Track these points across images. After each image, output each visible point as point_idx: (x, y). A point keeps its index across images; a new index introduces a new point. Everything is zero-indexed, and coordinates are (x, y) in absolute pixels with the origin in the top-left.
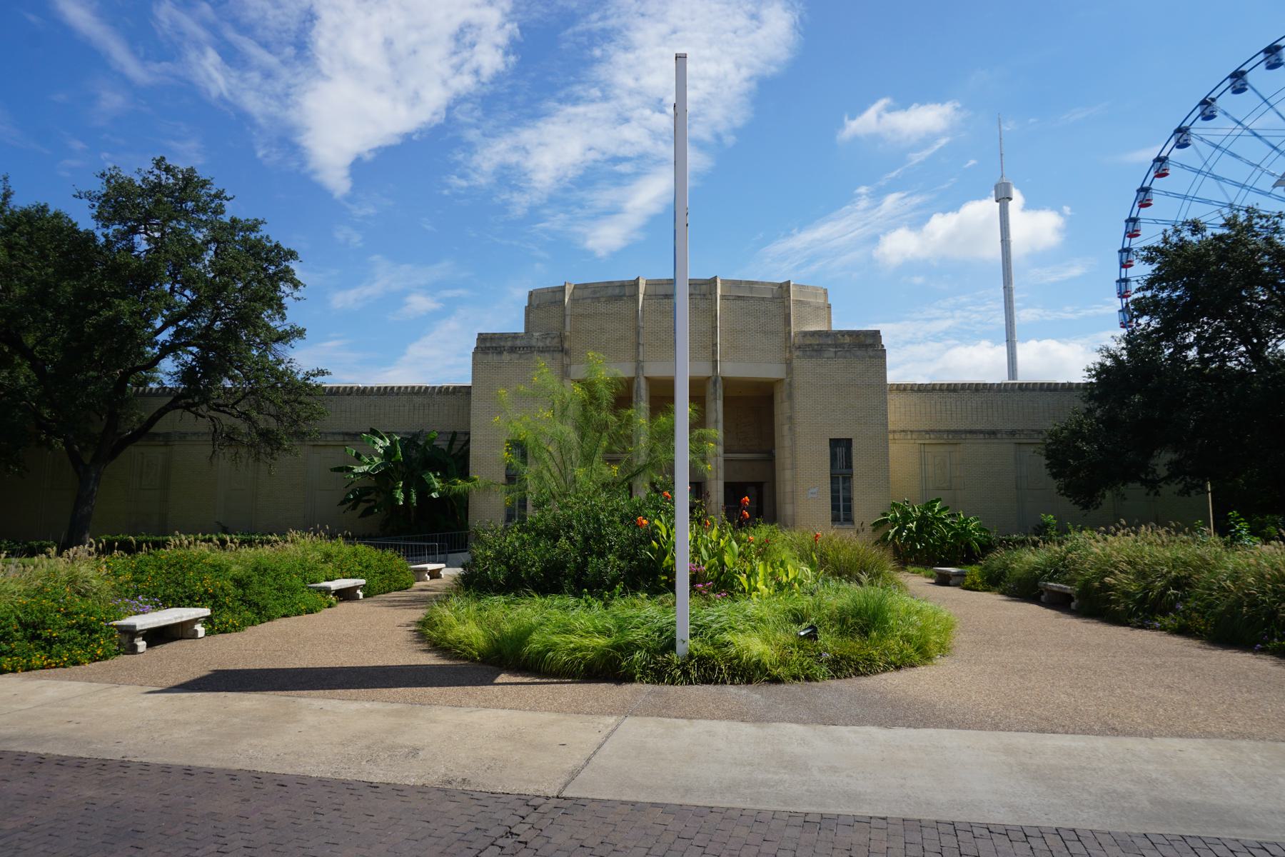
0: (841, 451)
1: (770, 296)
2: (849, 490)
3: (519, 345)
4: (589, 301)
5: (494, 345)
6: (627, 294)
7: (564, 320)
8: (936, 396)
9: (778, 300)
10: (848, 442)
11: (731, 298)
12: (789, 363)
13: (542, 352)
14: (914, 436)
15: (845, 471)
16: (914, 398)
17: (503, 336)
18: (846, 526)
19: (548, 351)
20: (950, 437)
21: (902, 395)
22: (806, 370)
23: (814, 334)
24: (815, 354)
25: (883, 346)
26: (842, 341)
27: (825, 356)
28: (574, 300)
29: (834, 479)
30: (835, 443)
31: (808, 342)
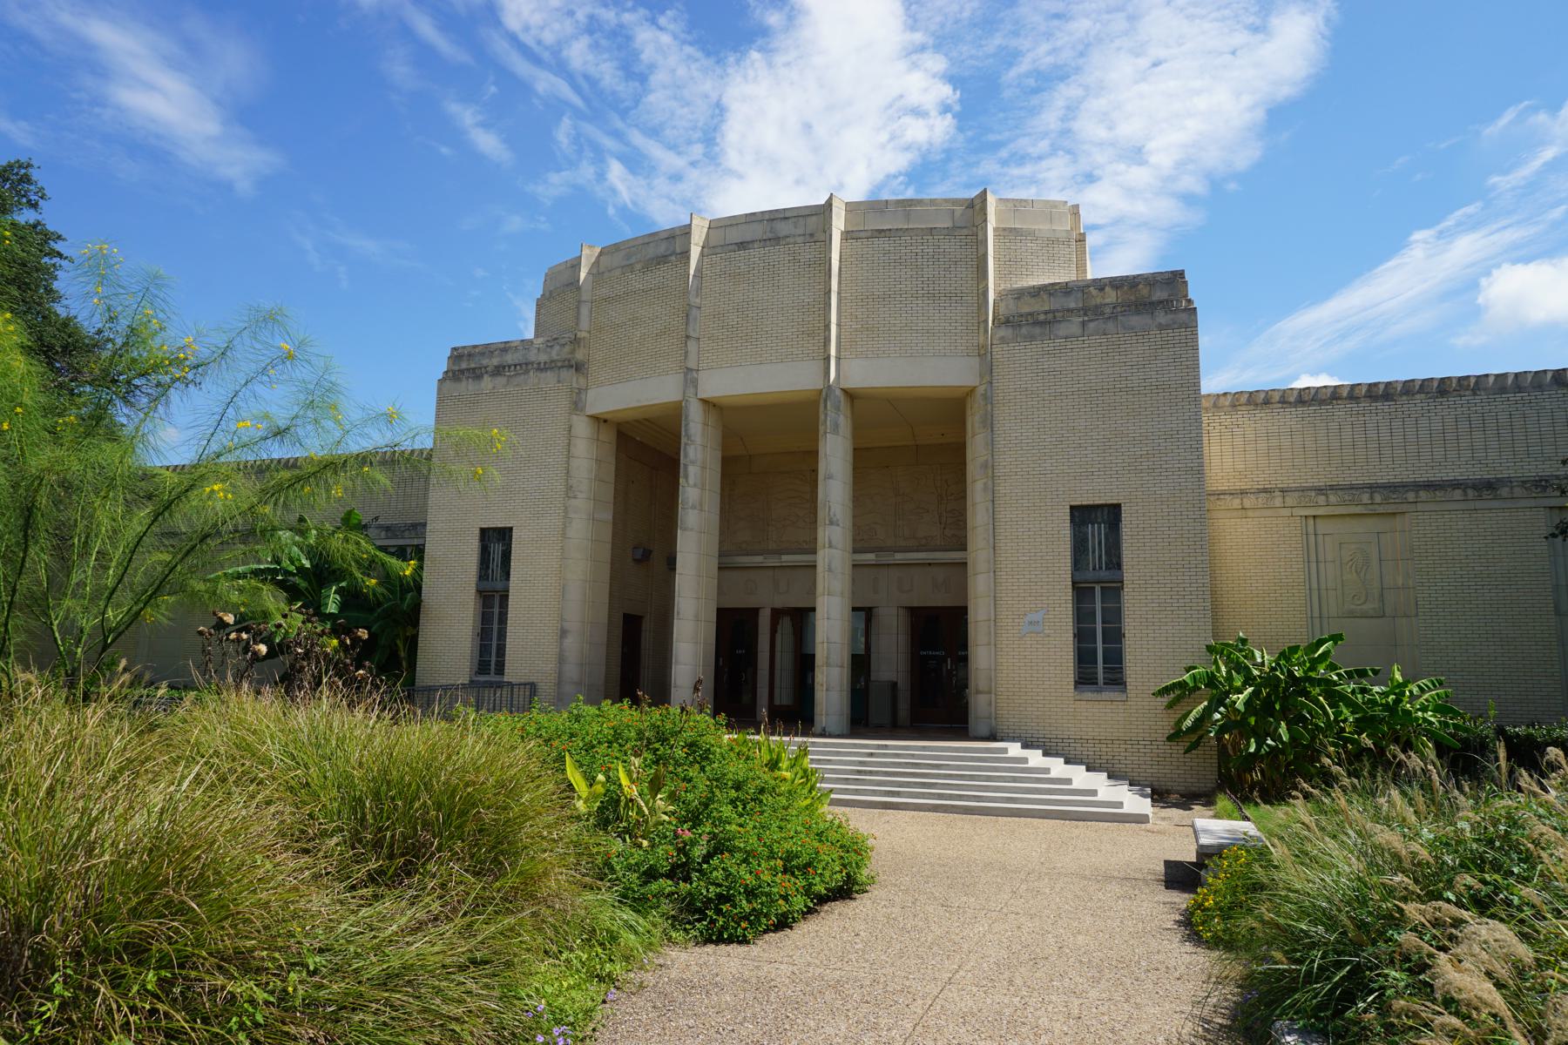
0: (1096, 533)
1: (949, 224)
2: (1114, 617)
3: (510, 362)
5: (473, 366)
6: (678, 251)
7: (578, 313)
8: (1340, 411)
9: (965, 232)
10: (1112, 514)
11: (863, 235)
14: (1290, 501)
16: (1290, 418)
17: (488, 350)
18: (1106, 695)
21: (1259, 414)
23: (1037, 292)
24: (1037, 330)
25: (1190, 301)
26: (1099, 301)
27: (1061, 333)
28: (597, 271)
29: (1081, 592)
30: (1081, 515)
31: (1026, 309)
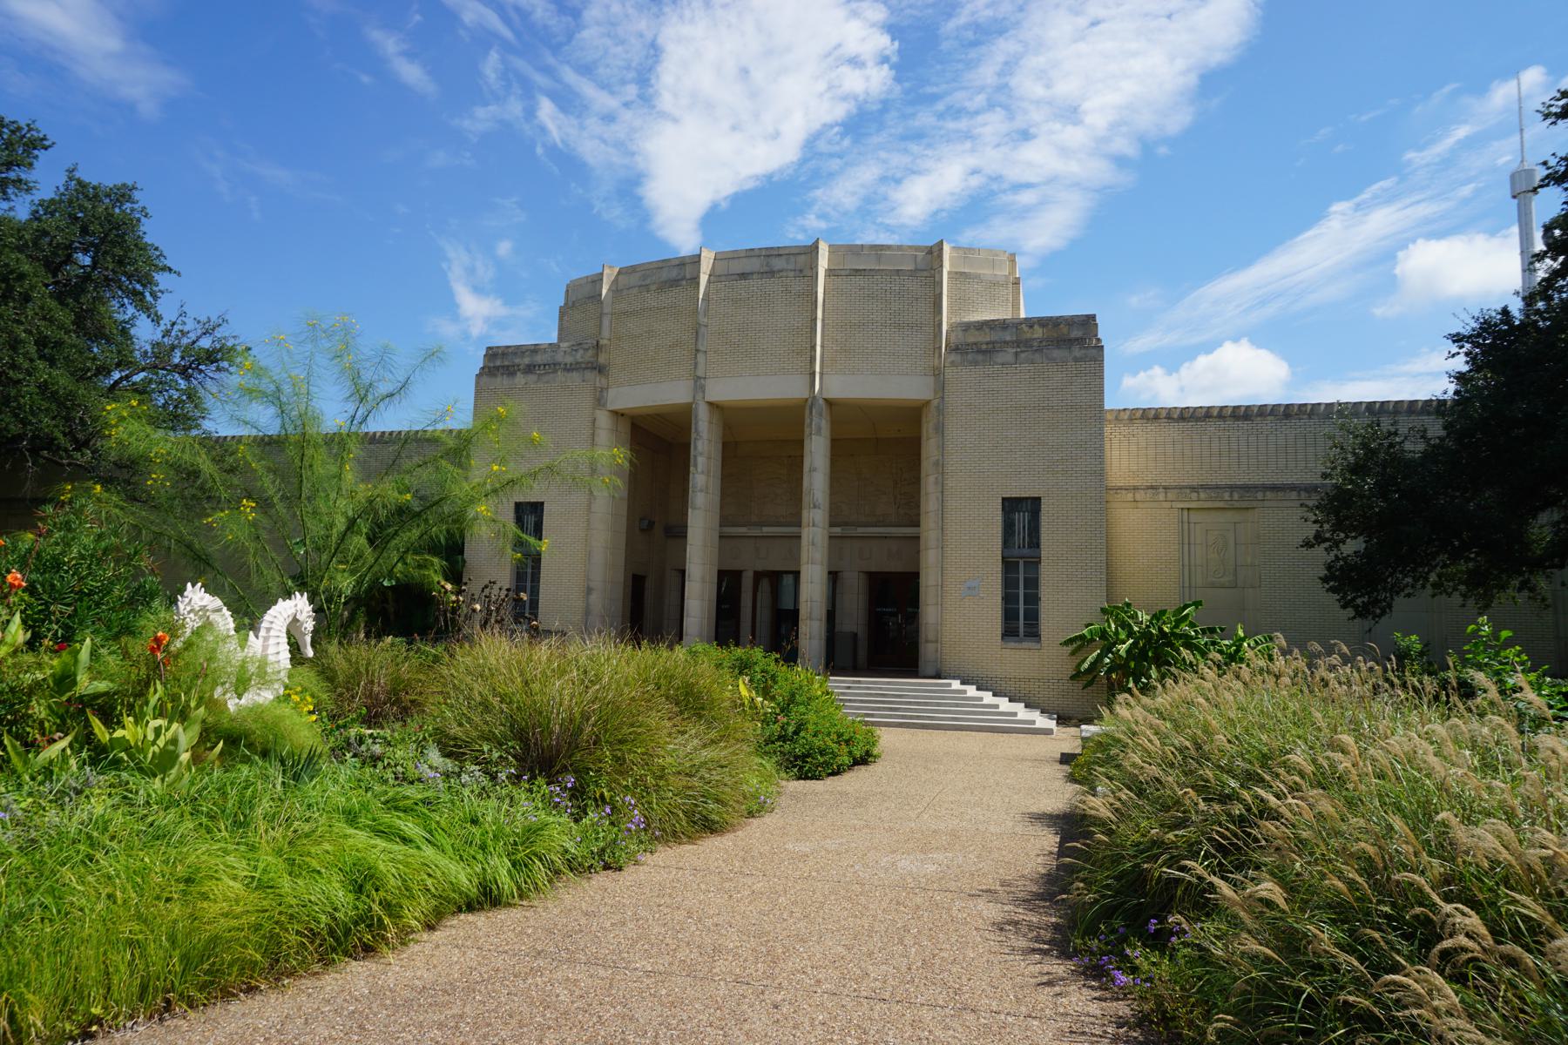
0: (1021, 519)
1: (911, 267)
2: (1033, 583)
3: (540, 362)
4: (635, 291)
5: (506, 363)
6: (688, 276)
7: (601, 321)
8: (1211, 427)
9: (925, 274)
10: (1032, 506)
11: (843, 273)
12: (937, 373)
13: (568, 370)
14: (1171, 495)
15: (1026, 551)
16: (1174, 431)
17: (519, 350)
18: (1025, 645)
19: (577, 369)
20: (1236, 496)
21: (1151, 427)
22: (965, 381)
23: (982, 326)
24: (980, 357)
25: (1099, 340)
26: (1028, 336)
27: (999, 360)
28: (616, 289)
29: (1009, 566)
30: (1011, 506)
31: (971, 340)
